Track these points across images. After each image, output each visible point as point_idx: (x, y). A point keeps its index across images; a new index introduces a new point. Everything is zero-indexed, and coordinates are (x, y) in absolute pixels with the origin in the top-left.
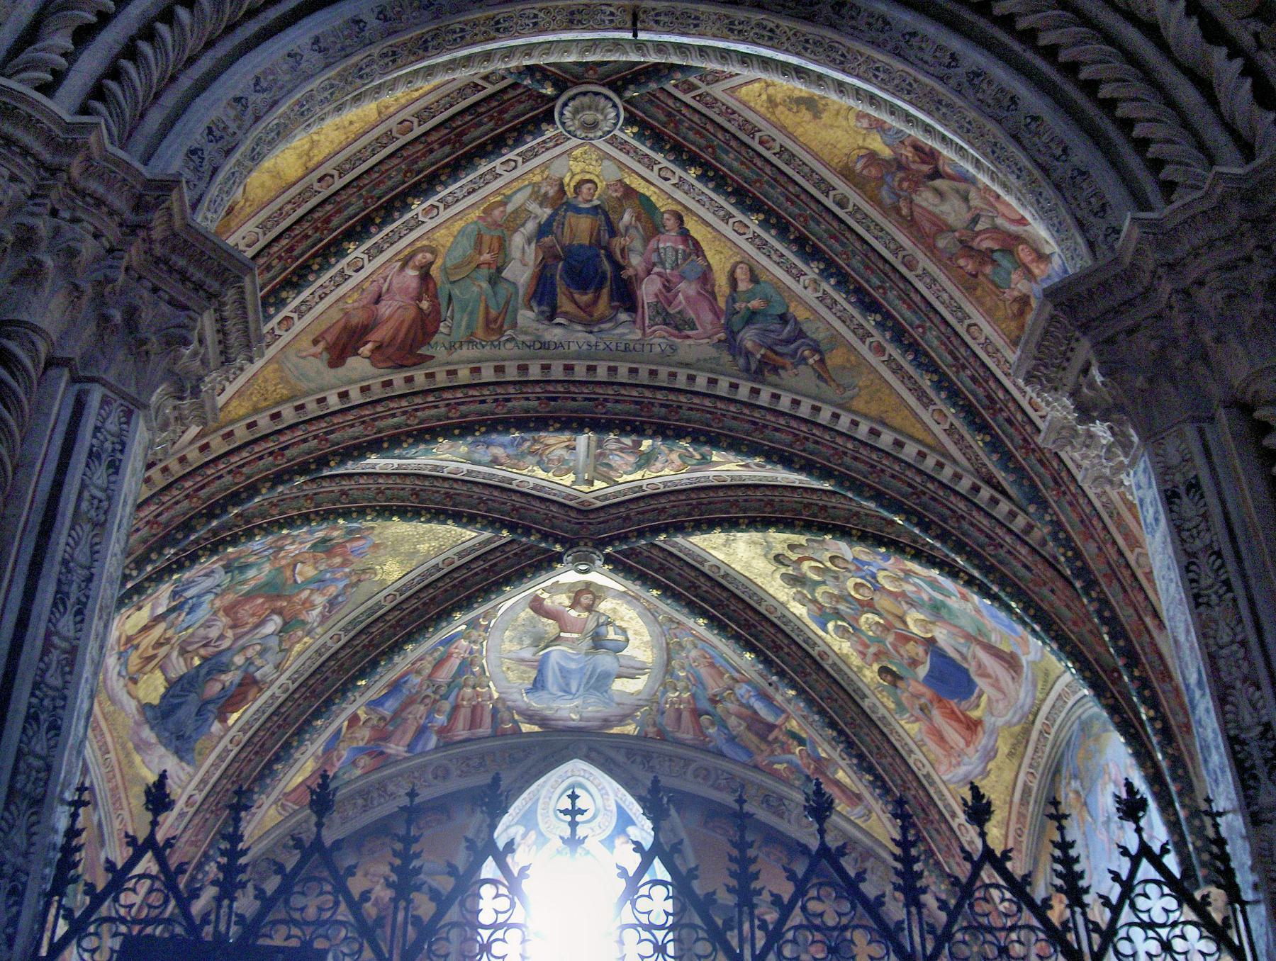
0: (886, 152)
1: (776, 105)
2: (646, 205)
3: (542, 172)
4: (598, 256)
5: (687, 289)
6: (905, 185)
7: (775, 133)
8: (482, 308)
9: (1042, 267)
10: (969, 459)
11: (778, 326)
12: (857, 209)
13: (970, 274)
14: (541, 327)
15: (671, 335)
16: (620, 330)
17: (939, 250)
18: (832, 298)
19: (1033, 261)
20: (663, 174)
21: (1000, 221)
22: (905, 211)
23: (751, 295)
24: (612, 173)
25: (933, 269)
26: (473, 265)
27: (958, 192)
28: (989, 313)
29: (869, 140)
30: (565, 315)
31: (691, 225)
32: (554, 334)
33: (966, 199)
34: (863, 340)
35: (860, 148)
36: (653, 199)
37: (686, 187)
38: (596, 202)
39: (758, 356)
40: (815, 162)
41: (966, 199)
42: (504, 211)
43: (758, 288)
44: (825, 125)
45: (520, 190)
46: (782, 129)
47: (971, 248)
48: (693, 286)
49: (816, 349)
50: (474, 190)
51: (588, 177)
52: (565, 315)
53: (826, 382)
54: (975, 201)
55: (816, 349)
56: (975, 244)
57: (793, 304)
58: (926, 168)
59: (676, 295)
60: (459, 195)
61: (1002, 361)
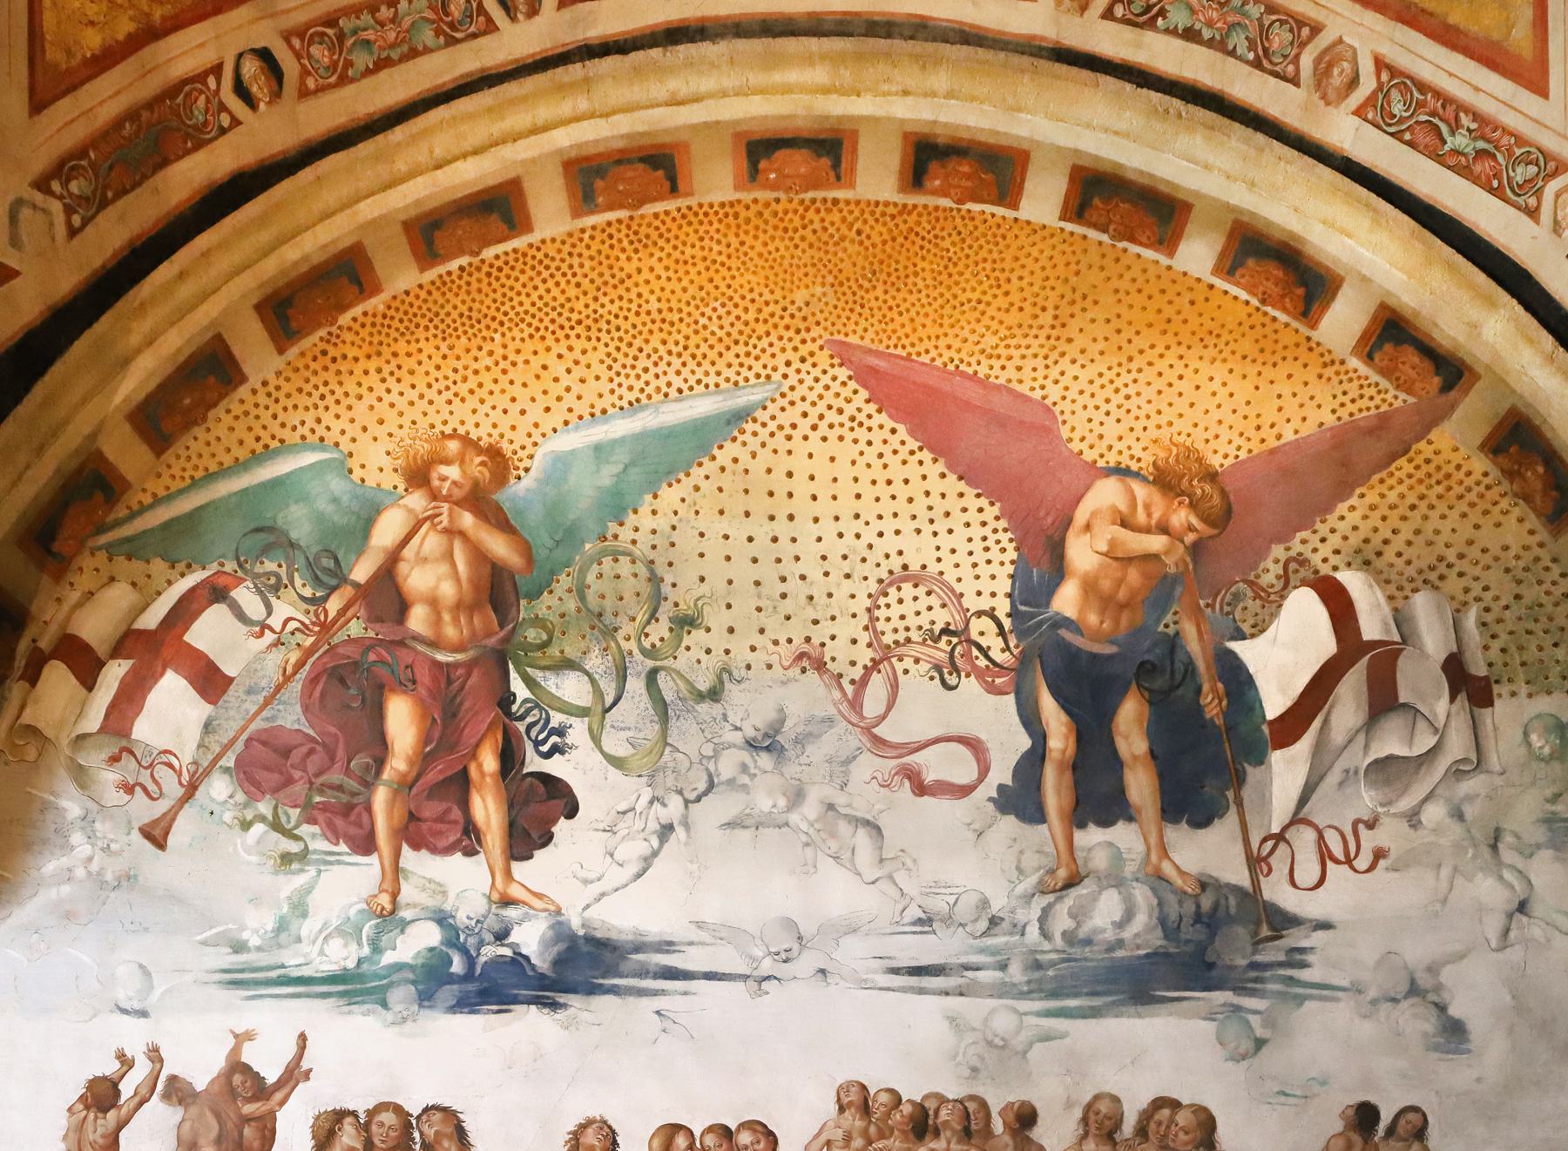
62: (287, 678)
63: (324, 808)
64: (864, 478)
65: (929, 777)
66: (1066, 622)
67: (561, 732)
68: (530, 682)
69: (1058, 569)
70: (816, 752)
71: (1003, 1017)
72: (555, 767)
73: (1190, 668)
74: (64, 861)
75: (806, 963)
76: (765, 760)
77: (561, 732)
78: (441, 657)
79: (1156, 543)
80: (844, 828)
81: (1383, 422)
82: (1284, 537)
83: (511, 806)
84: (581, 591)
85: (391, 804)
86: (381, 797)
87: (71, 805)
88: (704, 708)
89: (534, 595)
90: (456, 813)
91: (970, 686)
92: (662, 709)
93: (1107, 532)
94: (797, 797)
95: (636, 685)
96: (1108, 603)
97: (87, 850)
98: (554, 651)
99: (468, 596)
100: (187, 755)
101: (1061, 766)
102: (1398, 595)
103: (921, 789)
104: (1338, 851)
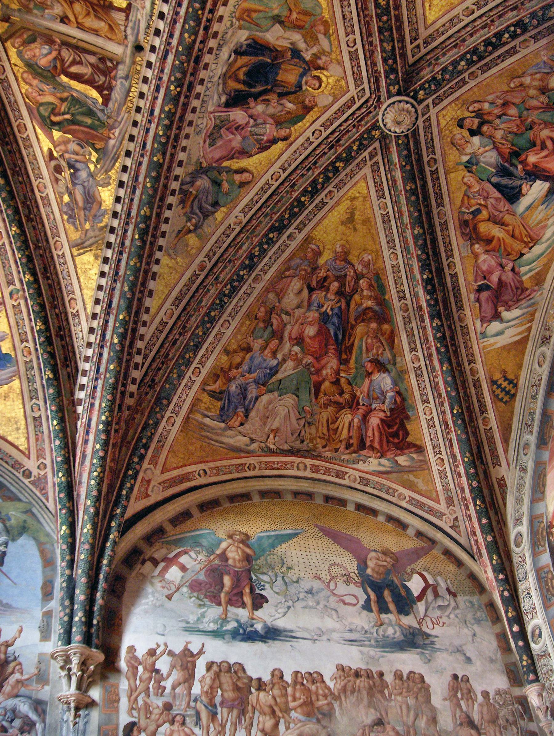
0: (321, 261)
1: (351, 201)
2: (299, 118)
3: (337, 60)
4: (267, 84)
5: (236, 141)
6: (303, 273)
7: (335, 199)
8: (261, 8)
9: (269, 355)
10: (150, 340)
11: (210, 201)
12: (287, 246)
13: (256, 316)
14: (232, 45)
15: (207, 131)
16: (216, 97)
17: (267, 295)
18: (230, 234)
19: (271, 349)
20: (317, 132)
21: (289, 327)
22: (287, 273)
23: (231, 183)
24: (323, 99)
25: (255, 294)
26: (292, 7)
27: (302, 302)
28: (238, 330)
29: (329, 251)
30: (235, 61)
31: (280, 145)
32: (225, 54)
33: (298, 307)
34: (206, 256)
35: (324, 247)
36: (300, 124)
37: (306, 145)
38: (304, 88)
39: (191, 190)
40: (316, 222)
41: (298, 307)
42: (320, 33)
43: (236, 187)
44: (338, 227)
45: (331, 45)
46: (338, 203)
47: (271, 314)
48: (238, 145)
49: (197, 227)
50: (344, 19)
51: (323, 85)
52: (235, 61)
53: (176, 237)
54: (298, 312)
55: (197, 227)
56: (273, 315)
57: (225, 210)
58: (314, 284)
59: (233, 134)
60: (346, 10)
61: (214, 345)
62: (201, 570)
63: (209, 596)
64: (324, 547)
65: (347, 602)
66: (368, 575)
67: (264, 586)
68: (256, 576)
69: (366, 566)
70: (321, 595)
71: (372, 652)
72: (263, 592)
73: (397, 586)
74: (147, 601)
75: (324, 638)
76: (309, 595)
77: (264, 586)
78: (236, 569)
79: (385, 563)
80: (329, 610)
81: (423, 548)
82: (410, 565)
83: (253, 599)
84: (266, 560)
85: (225, 598)
86: (222, 595)
87: (149, 589)
88: (295, 584)
89: (256, 560)
90: (240, 599)
91: (352, 585)
92: (286, 584)
93: (375, 561)
94: (318, 603)
95: (279, 579)
96: (377, 573)
97: (152, 599)
98: (261, 571)
99: (242, 559)
100: (177, 582)
101: (374, 602)
102: (434, 576)
103: (345, 604)
104: (435, 622)
